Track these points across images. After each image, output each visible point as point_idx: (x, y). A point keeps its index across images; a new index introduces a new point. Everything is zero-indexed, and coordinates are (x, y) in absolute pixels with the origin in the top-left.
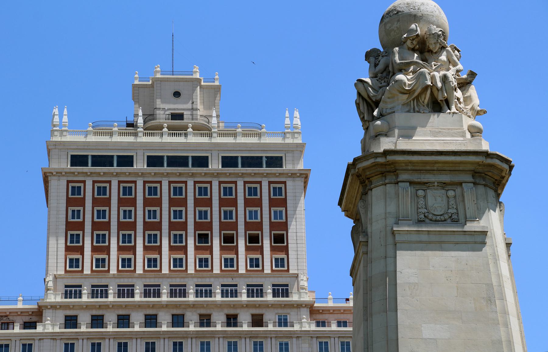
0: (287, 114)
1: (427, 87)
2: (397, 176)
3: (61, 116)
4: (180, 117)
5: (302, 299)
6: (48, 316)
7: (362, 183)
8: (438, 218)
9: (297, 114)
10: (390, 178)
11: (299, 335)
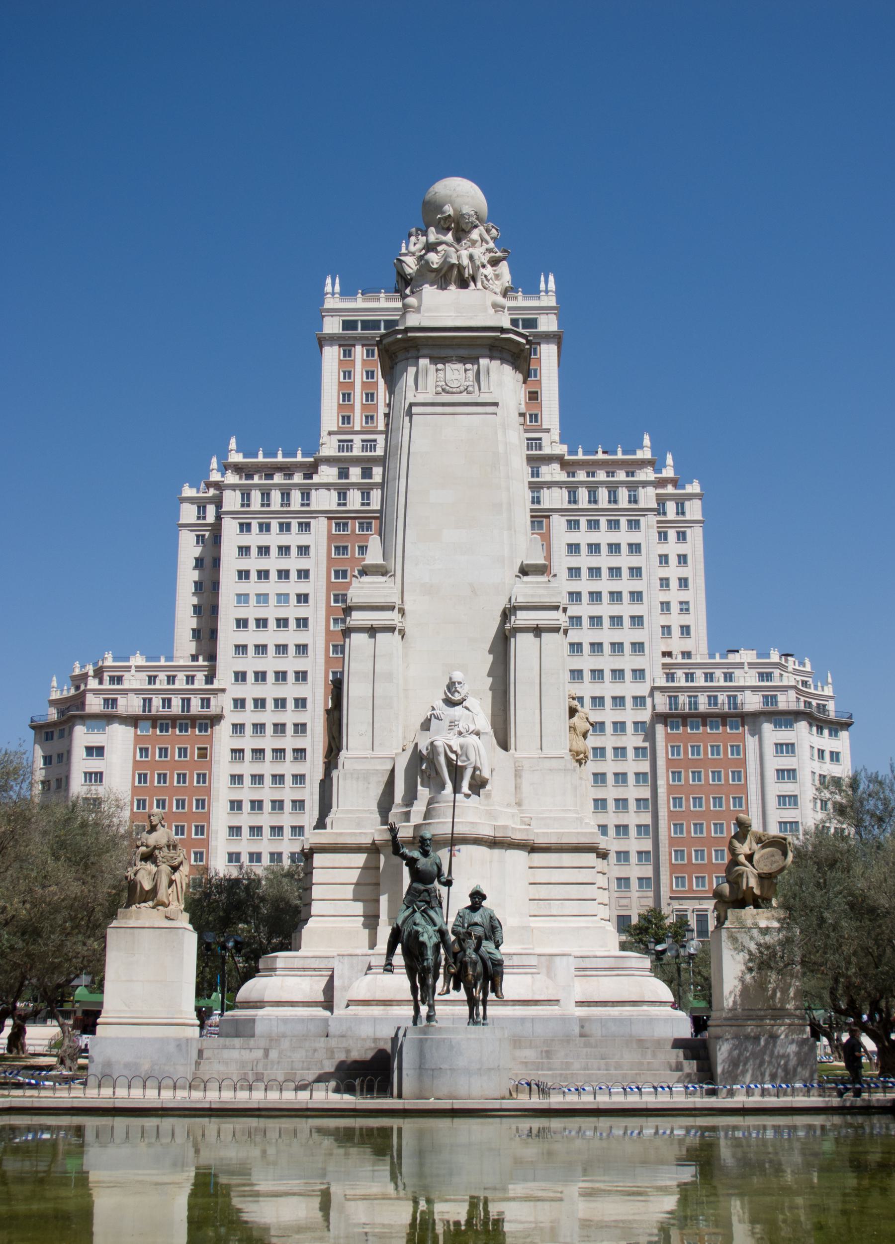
0: (542, 278)
1: (454, 265)
2: (418, 350)
5: (554, 452)
6: (323, 469)
7: (390, 358)
8: (454, 390)
9: (551, 278)
10: (413, 353)
11: (550, 485)
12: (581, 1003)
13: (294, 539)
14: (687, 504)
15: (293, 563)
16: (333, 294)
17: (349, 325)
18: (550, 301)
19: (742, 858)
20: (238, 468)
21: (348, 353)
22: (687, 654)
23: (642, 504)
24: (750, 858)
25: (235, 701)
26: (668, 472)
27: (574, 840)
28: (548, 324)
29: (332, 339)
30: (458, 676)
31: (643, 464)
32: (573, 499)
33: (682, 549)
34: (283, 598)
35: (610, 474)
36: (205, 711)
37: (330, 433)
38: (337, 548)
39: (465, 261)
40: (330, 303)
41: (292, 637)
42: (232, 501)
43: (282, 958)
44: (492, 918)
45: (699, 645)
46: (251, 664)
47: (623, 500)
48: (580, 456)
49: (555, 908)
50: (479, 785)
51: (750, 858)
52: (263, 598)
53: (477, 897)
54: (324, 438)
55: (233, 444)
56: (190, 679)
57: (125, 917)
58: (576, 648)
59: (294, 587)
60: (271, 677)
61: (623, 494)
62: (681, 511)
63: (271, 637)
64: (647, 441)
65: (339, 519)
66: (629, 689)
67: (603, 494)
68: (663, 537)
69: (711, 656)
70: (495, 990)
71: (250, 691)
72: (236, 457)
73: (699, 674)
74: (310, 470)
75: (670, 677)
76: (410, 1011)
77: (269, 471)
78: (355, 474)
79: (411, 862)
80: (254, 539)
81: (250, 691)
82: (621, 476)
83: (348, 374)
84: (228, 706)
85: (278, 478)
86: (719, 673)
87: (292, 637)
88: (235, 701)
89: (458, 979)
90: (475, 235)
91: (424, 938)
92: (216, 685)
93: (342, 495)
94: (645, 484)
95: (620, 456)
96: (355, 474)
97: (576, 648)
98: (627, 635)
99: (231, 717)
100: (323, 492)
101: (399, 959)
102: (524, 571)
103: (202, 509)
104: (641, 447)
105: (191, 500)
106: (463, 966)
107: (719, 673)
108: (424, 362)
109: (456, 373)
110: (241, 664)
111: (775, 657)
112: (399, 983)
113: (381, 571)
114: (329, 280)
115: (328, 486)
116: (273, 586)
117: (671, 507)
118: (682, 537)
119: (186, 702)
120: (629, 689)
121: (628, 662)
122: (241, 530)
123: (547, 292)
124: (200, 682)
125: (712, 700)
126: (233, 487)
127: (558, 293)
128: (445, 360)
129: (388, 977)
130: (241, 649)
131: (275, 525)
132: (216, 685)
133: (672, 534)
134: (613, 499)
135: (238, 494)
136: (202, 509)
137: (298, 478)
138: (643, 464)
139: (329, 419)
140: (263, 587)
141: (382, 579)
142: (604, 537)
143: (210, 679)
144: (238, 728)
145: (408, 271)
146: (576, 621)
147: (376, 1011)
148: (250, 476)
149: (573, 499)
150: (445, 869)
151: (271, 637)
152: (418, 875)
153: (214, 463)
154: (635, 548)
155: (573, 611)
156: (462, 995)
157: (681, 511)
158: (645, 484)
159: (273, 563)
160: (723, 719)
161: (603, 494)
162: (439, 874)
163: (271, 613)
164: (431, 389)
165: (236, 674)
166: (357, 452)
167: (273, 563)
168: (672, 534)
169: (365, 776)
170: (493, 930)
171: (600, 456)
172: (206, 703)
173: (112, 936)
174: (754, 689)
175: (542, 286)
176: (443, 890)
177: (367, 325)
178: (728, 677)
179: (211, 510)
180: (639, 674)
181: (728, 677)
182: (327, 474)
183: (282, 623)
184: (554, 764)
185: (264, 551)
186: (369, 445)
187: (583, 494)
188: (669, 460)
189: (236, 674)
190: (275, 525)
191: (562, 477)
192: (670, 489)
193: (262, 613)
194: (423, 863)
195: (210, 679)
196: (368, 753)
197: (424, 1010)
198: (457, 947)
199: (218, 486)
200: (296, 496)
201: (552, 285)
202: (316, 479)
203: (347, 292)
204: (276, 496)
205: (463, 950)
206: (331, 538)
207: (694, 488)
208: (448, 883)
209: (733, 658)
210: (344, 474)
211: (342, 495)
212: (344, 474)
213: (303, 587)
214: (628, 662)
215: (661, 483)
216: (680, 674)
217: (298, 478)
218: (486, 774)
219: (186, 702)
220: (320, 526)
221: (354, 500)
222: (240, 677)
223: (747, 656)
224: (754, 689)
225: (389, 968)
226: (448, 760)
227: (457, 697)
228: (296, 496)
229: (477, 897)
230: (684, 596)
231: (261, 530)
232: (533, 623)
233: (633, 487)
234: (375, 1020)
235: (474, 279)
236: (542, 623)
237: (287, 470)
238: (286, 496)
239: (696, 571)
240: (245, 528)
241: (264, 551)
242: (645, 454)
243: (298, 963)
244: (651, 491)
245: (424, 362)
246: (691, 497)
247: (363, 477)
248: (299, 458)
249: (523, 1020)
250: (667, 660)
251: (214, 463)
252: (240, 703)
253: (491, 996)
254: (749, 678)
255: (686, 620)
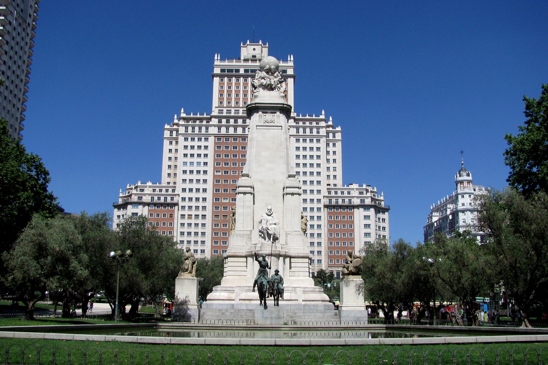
3: (218, 57)
4: (255, 56)
6: (213, 119)
9: (292, 56)
12: (303, 301)
13: (203, 143)
14: (336, 134)
15: (202, 152)
16: (217, 60)
17: (223, 71)
18: (291, 64)
19: (349, 262)
20: (184, 119)
21: (222, 80)
22: (335, 185)
23: (321, 134)
24: (351, 262)
25: (182, 198)
26: (330, 123)
27: (302, 255)
28: (290, 72)
29: (217, 75)
30: (269, 207)
31: (321, 120)
32: (298, 132)
33: (334, 149)
34: (199, 163)
35: (311, 123)
36: (172, 202)
37: (216, 107)
38: (217, 147)
39: (273, 83)
40: (216, 63)
41: (202, 177)
42: (182, 130)
43: (218, 287)
44: (281, 278)
45: (339, 181)
46: (188, 186)
47: (315, 133)
48: (301, 117)
49: (297, 274)
50: (275, 239)
51: (351, 262)
52: (192, 163)
53: (277, 272)
54: (214, 109)
55: (182, 111)
56: (167, 191)
57: (181, 275)
58: (305, 200)
59: (202, 160)
60: (194, 190)
61: (315, 130)
62: (334, 136)
63: (195, 177)
64: (323, 112)
65: (218, 137)
66: (315, 196)
67: (308, 130)
68: (328, 145)
69: (344, 186)
70: (281, 297)
71: (187, 195)
72: (183, 115)
73: (339, 192)
74: (209, 120)
75: (330, 193)
76: (259, 302)
77: (195, 120)
78: (224, 121)
79: (260, 263)
80: (189, 143)
81: (187, 195)
82: (314, 124)
83: (222, 87)
84: (180, 200)
85: (198, 122)
86: (346, 192)
87: (202, 177)
88: (182, 198)
89: (271, 294)
90: (275, 75)
91: (264, 283)
92: (176, 193)
93: (219, 129)
94: (322, 127)
95: (314, 117)
96: (224, 121)
97: (305, 200)
98: (315, 178)
99: (181, 204)
100: (213, 127)
101: (256, 288)
102: (290, 176)
103: (171, 132)
104: (322, 115)
105: (168, 129)
106: (273, 290)
107: (346, 192)
108: (260, 113)
109: (269, 116)
110: (184, 186)
111: (364, 186)
112: (256, 295)
113: (247, 176)
114: (216, 55)
115: (215, 126)
116: (195, 159)
117: (331, 135)
118: (334, 145)
119: (166, 199)
120: (315, 196)
121: (315, 187)
122: (185, 140)
123: (290, 61)
124: (170, 192)
125: (343, 201)
126: (182, 125)
127: (294, 61)
128: (266, 113)
129: (254, 293)
130: (184, 181)
131: (196, 138)
132: (176, 193)
133: (331, 144)
134: (311, 132)
135: (184, 128)
136: (171, 132)
137: (204, 122)
138: (321, 120)
139: (215, 102)
140: (192, 160)
141: (248, 178)
142: (308, 145)
143: (173, 191)
144: (183, 207)
145: (255, 84)
146: (305, 191)
147: (247, 302)
148: (188, 122)
149: (298, 132)
150: (269, 265)
151: (195, 177)
152: (261, 266)
153: (176, 117)
154: (318, 149)
155: (304, 187)
156: (272, 298)
157: (334, 136)
158: (322, 127)
159: (196, 152)
160: (347, 207)
161: (308, 130)
162: (267, 266)
163: (195, 168)
164: (263, 121)
165: (183, 189)
166: (225, 114)
167: (196, 152)
168: (331, 144)
169: (242, 236)
170: (281, 281)
171: (307, 117)
172: (172, 199)
173: (177, 281)
174: (357, 197)
175: (289, 59)
176: (268, 270)
177: (229, 71)
178: (349, 193)
179: (174, 133)
180: (319, 191)
181: (349, 193)
182: (215, 121)
183: (198, 172)
184: (297, 233)
185: (192, 147)
186: (229, 112)
187: (301, 130)
188: (331, 119)
189: (183, 189)
190: (196, 138)
191: (294, 124)
192: (331, 129)
193: (191, 169)
194: (263, 263)
195: (173, 191)
196: (242, 229)
197: (263, 302)
198: (271, 285)
199: (177, 125)
200: (204, 129)
201: (292, 59)
202: (211, 123)
203: (222, 59)
204: (197, 129)
205: (273, 286)
206: (215, 143)
207: (339, 129)
208: (270, 268)
209: (351, 187)
210: (220, 122)
211: (219, 129)
212: (220, 122)
213: (205, 160)
214: (315, 187)
215: (328, 126)
216: (333, 192)
217: (204, 122)
218: (278, 236)
219: (166, 199)
220: (212, 139)
221: (223, 130)
222: (184, 190)
223: (355, 186)
224: (357, 197)
225: (254, 291)
226: (267, 232)
227: (269, 213)
228: (204, 129)
229: (277, 272)
230: (335, 165)
231: (192, 140)
232: (291, 192)
233: (318, 128)
234: (247, 305)
235: (275, 88)
236: (294, 192)
237: (201, 120)
238: (200, 129)
239: (339, 157)
240: (186, 139)
241: (192, 147)
242: (322, 117)
243: (224, 289)
244: (324, 129)
245: (260, 113)
246: (338, 132)
247: (227, 123)
248: (205, 116)
249: (288, 305)
250: (329, 187)
251: (176, 117)
252: (184, 199)
253: (280, 298)
254: (355, 193)
255: (335, 173)
